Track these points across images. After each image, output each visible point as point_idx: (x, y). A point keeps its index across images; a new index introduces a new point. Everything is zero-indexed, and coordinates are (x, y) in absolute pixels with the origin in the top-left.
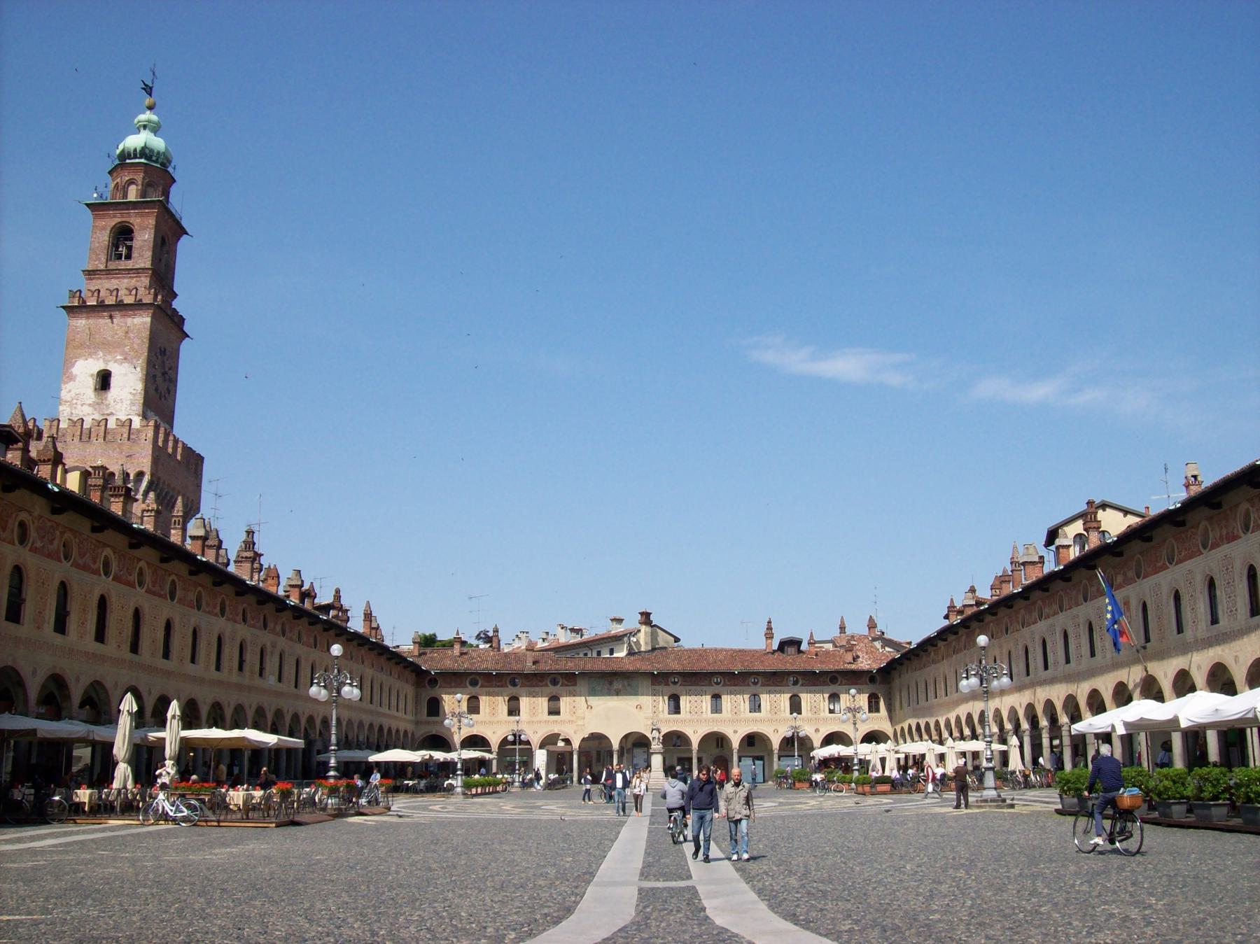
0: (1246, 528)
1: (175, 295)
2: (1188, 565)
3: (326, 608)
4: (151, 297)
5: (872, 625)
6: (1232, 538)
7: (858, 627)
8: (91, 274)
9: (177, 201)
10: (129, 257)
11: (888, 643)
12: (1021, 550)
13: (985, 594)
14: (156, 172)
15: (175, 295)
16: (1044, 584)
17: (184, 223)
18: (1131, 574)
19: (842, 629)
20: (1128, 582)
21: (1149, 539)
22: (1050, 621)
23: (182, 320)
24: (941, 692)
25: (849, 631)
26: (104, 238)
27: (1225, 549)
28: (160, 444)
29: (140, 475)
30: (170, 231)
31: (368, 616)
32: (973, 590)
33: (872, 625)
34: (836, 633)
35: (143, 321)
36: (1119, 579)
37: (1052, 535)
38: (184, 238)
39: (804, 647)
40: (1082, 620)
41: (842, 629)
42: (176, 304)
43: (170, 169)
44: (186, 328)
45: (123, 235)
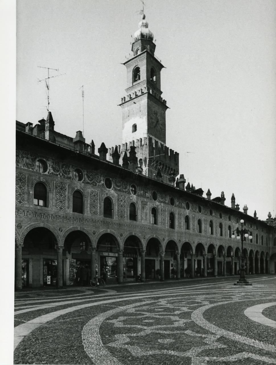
1: (161, 93)
3: (217, 199)
4: (146, 90)
8: (128, 90)
9: (157, 55)
10: (139, 79)
14: (147, 43)
15: (161, 93)
17: (162, 63)
23: (165, 102)
26: (131, 75)
28: (154, 146)
29: (146, 159)
30: (155, 67)
31: (233, 198)
35: (144, 101)
38: (163, 69)
42: (162, 96)
43: (154, 42)
44: (167, 105)
45: (136, 72)
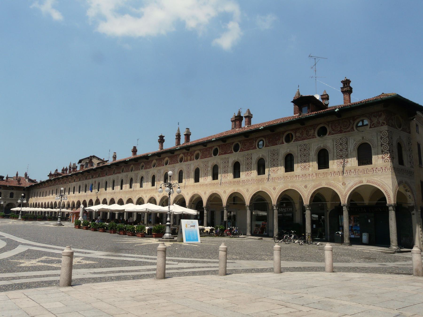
0: (123, 171)
2: (110, 176)
5: (26, 175)
6: (120, 173)
7: (22, 175)
11: (30, 180)
12: (72, 165)
13: (60, 171)
16: (76, 174)
18: (97, 175)
19: (17, 175)
20: (96, 177)
21: (103, 169)
22: (77, 182)
24: (44, 195)
25: (19, 176)
27: (118, 175)
32: (57, 170)
33: (26, 175)
34: (15, 176)
36: (95, 176)
37: (80, 162)
39: (5, 179)
40: (84, 184)
41: (17, 175)
